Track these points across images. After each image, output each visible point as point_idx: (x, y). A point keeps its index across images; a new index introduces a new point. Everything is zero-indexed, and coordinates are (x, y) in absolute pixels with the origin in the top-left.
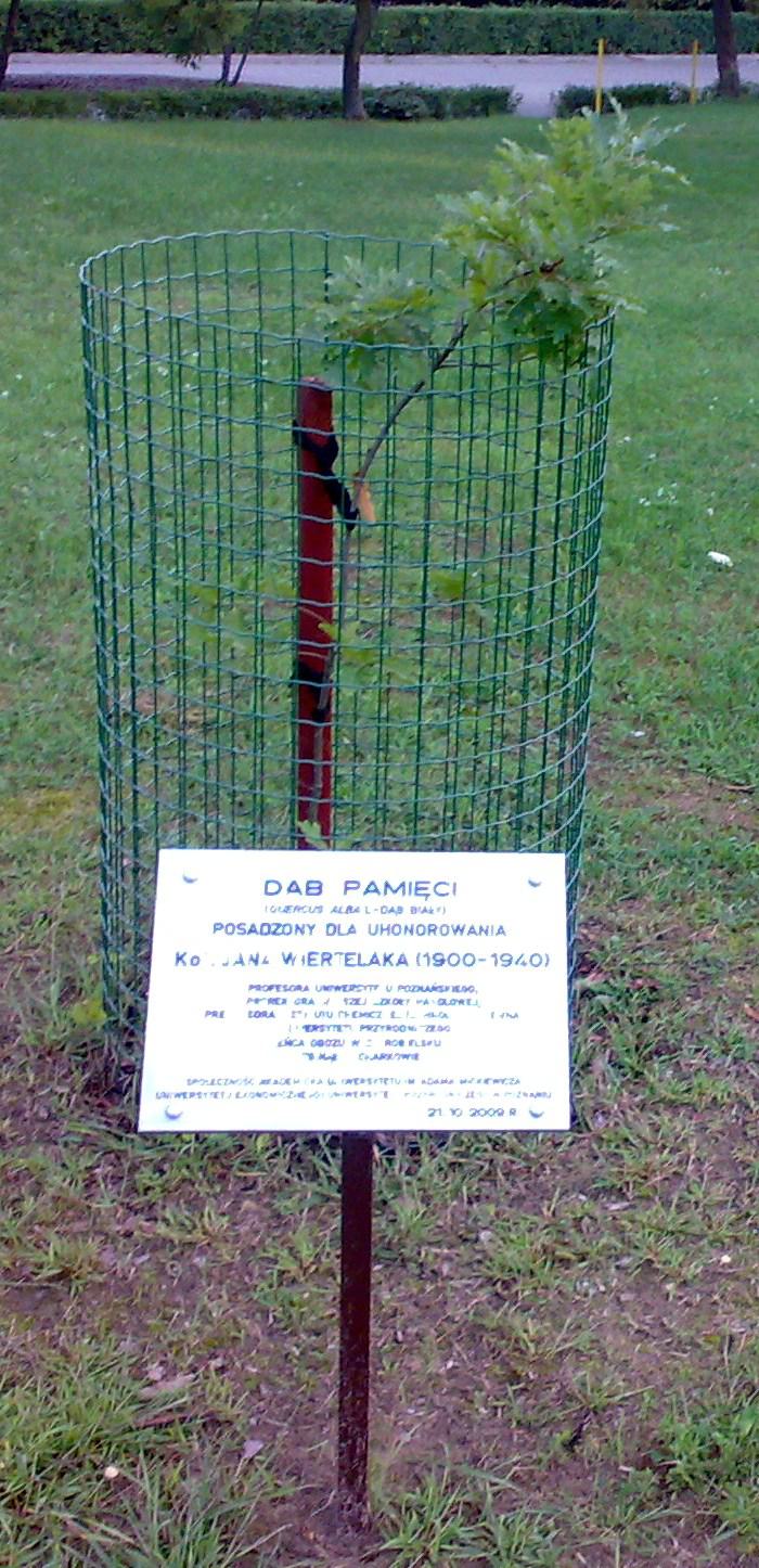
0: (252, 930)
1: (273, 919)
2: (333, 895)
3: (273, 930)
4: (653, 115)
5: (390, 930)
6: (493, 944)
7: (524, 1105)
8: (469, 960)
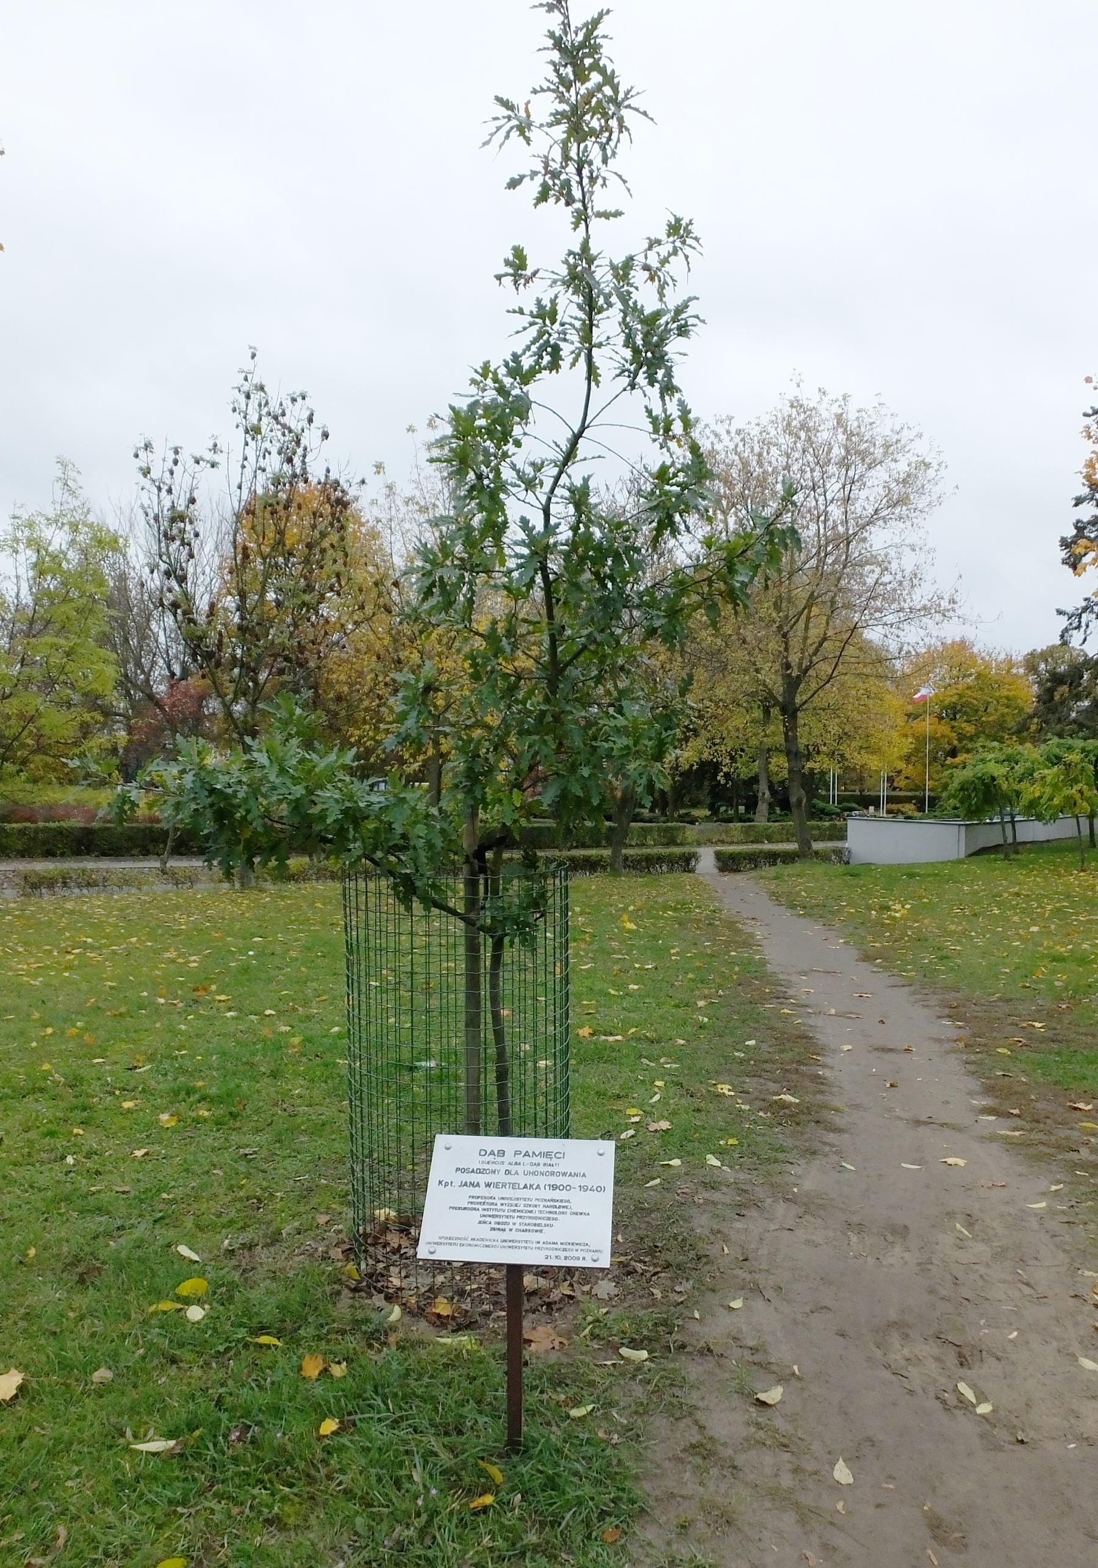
0: (473, 1171)
1: (480, 1166)
2: (509, 1157)
3: (480, 1171)
4: (470, 846)
5: (534, 1173)
6: (582, 1181)
7: (589, 1256)
8: (567, 1188)
